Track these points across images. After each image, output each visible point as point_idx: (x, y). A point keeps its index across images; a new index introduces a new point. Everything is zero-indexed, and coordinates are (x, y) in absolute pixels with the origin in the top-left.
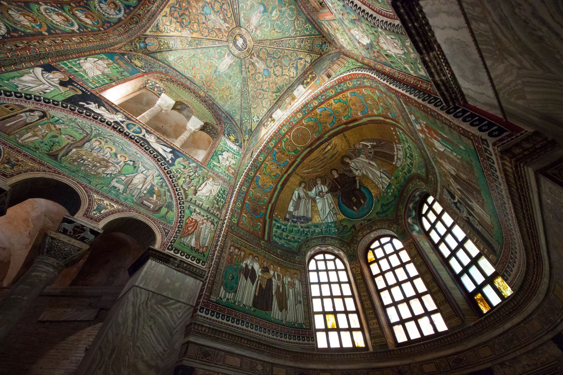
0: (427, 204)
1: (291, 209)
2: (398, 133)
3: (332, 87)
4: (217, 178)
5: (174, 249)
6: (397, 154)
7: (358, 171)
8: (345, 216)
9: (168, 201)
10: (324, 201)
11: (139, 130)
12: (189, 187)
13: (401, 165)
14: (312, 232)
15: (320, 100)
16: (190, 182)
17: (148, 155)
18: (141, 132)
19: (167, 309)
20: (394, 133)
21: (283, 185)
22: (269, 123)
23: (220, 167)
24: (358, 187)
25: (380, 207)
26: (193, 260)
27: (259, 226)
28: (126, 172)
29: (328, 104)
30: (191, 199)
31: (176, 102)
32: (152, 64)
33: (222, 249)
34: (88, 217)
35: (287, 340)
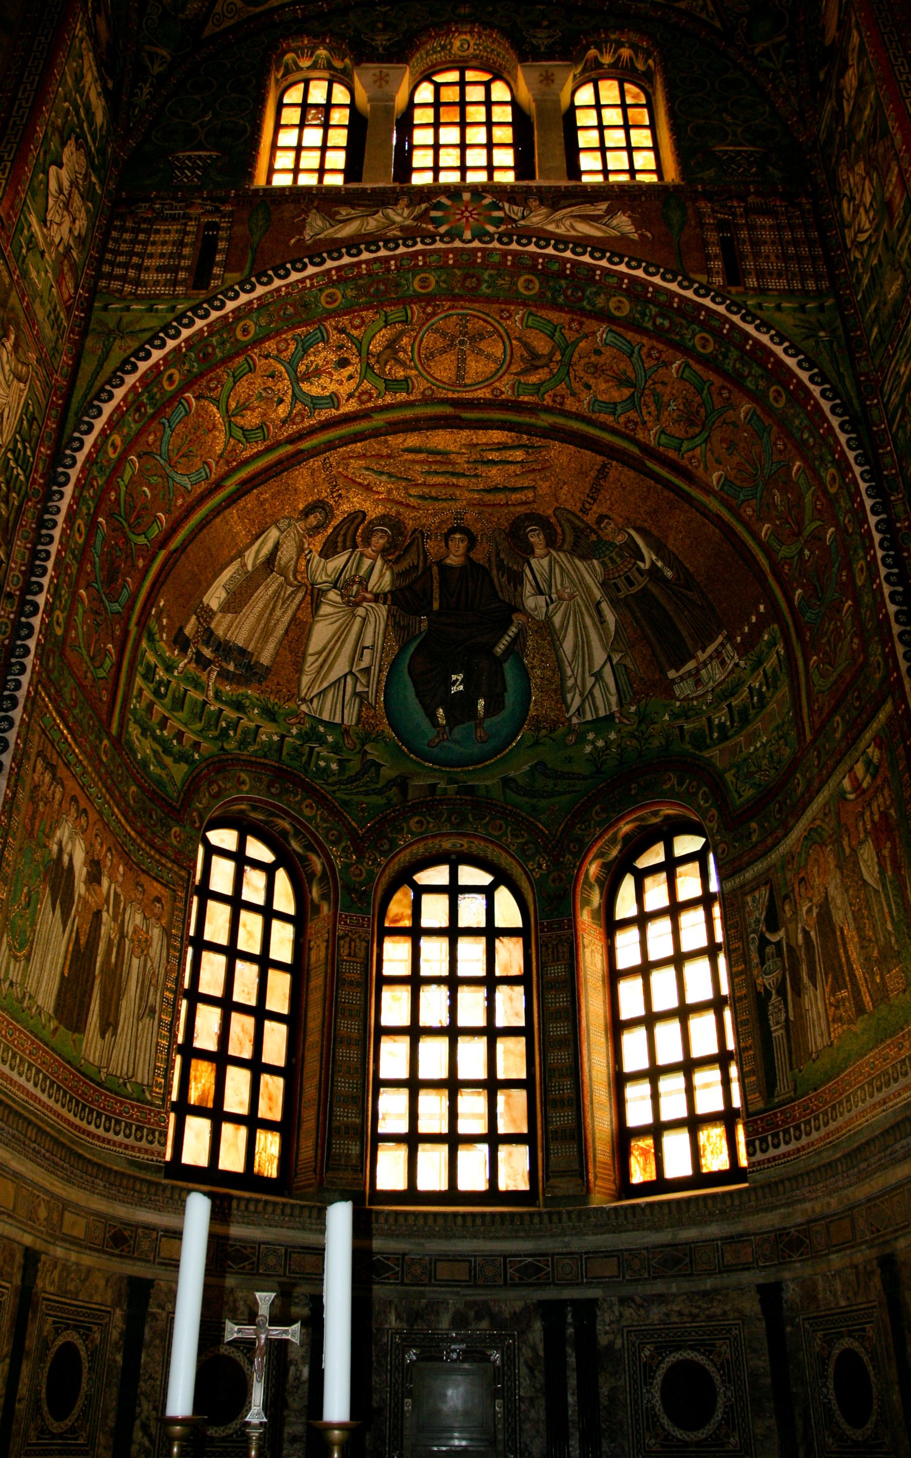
0: (669, 850)
1: (215, 598)
2: (766, 637)
3: (716, 333)
6: (705, 664)
7: (541, 600)
8: (390, 724)
10: (348, 626)
13: (686, 698)
14: (246, 732)
15: (643, 315)
20: (754, 619)
21: (246, 487)
22: (305, 63)
24: (500, 649)
25: (527, 768)
29: (655, 354)
35: (101, 1132)
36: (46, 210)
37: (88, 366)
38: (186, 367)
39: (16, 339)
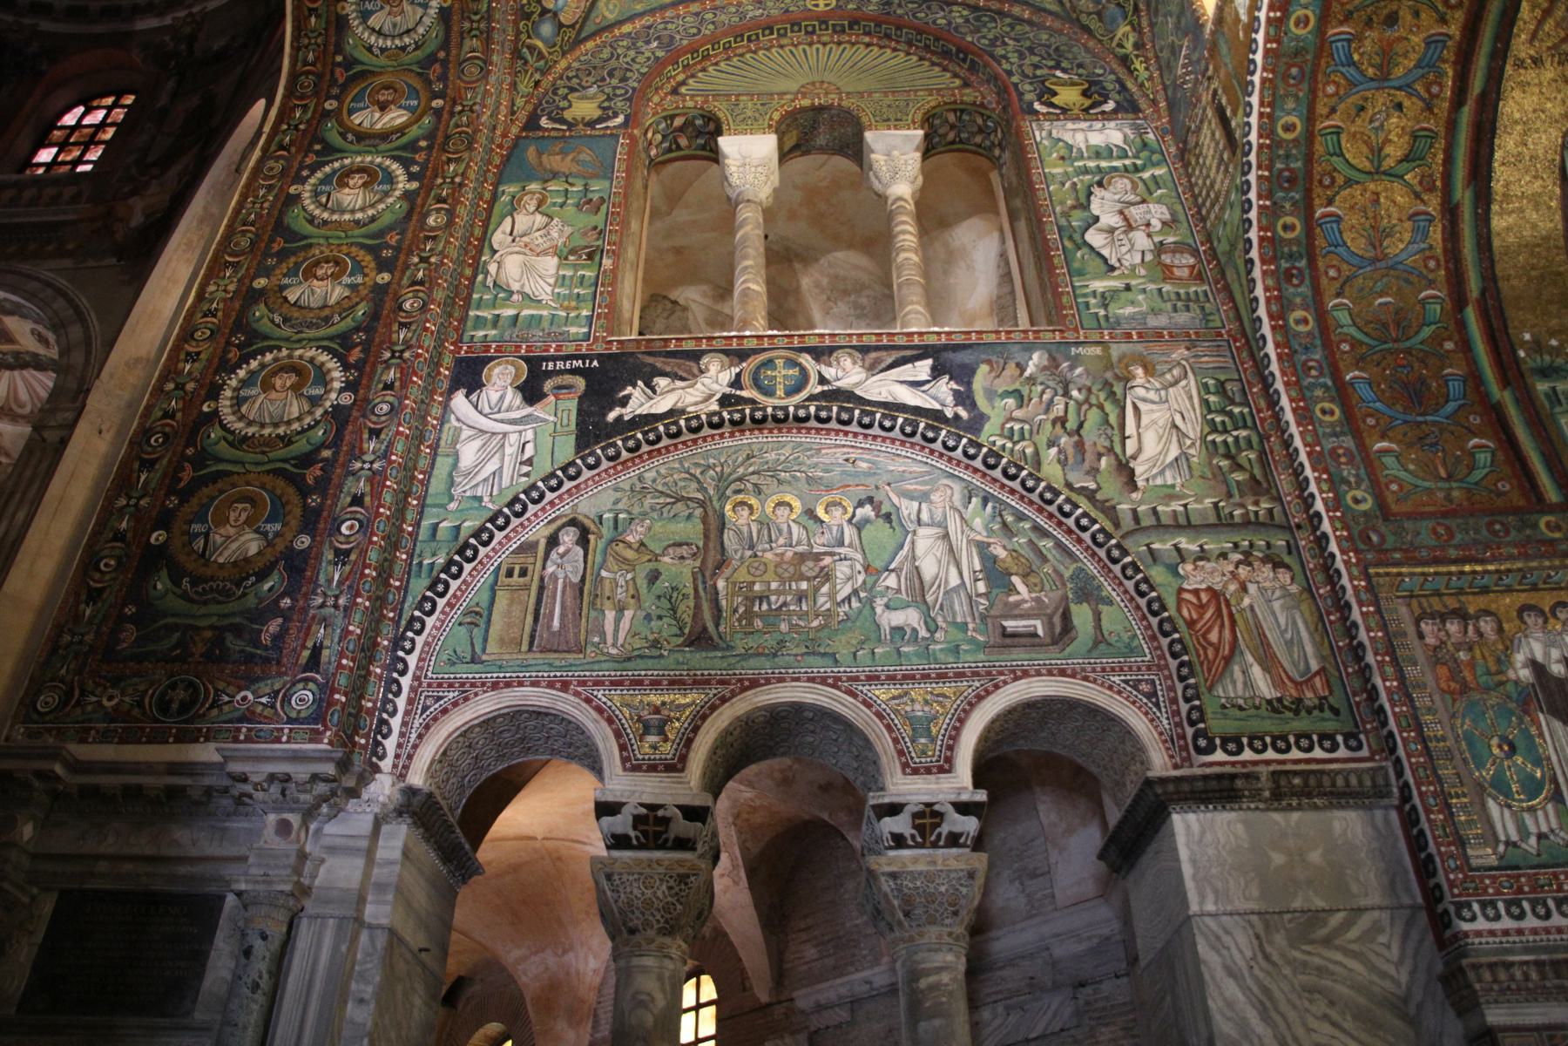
4: (1156, 348)
5: (1218, 741)
9: (1067, 574)
11: (794, 372)
12: (1094, 472)
16: (1080, 446)
17: (884, 439)
18: (804, 376)
19: (1338, 948)
23: (1128, 288)
26: (1310, 749)
27: (1483, 458)
28: (886, 557)
30: (1134, 511)
31: (776, 132)
32: (613, 63)
33: (1391, 650)
34: (916, 772)
36: (1105, 260)
37: (1238, 297)
38: (1288, 205)
39: (1145, 367)
